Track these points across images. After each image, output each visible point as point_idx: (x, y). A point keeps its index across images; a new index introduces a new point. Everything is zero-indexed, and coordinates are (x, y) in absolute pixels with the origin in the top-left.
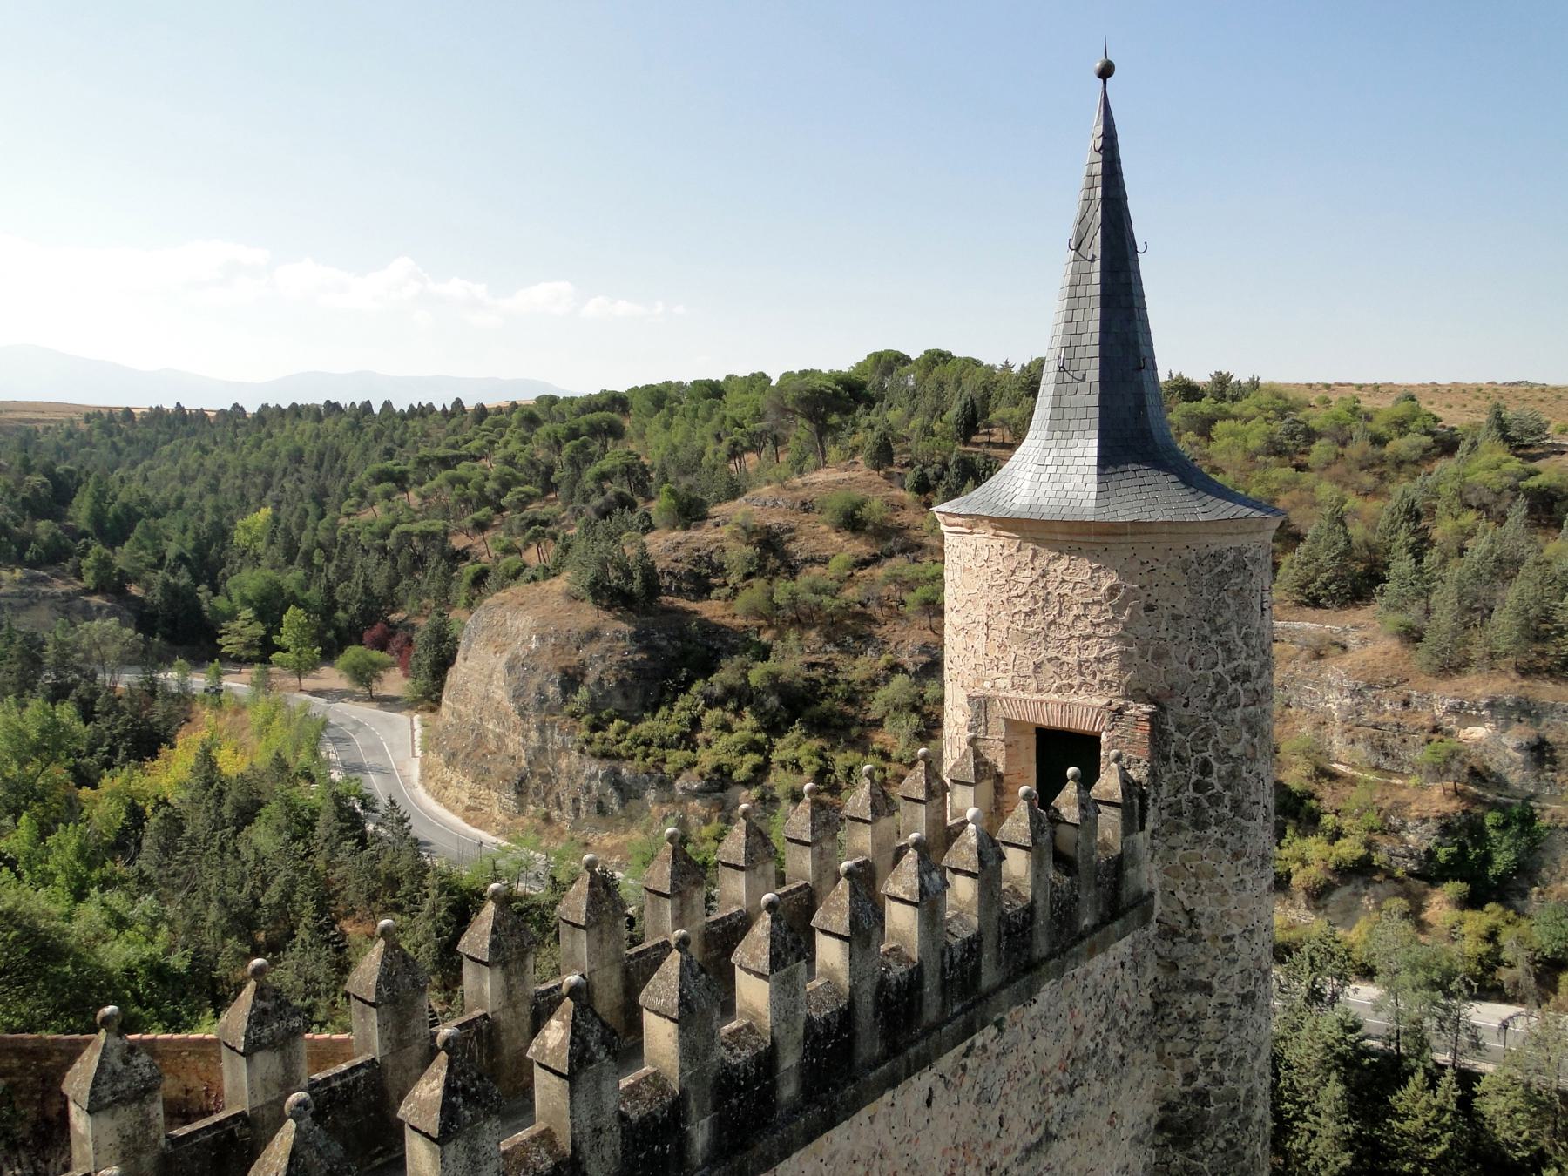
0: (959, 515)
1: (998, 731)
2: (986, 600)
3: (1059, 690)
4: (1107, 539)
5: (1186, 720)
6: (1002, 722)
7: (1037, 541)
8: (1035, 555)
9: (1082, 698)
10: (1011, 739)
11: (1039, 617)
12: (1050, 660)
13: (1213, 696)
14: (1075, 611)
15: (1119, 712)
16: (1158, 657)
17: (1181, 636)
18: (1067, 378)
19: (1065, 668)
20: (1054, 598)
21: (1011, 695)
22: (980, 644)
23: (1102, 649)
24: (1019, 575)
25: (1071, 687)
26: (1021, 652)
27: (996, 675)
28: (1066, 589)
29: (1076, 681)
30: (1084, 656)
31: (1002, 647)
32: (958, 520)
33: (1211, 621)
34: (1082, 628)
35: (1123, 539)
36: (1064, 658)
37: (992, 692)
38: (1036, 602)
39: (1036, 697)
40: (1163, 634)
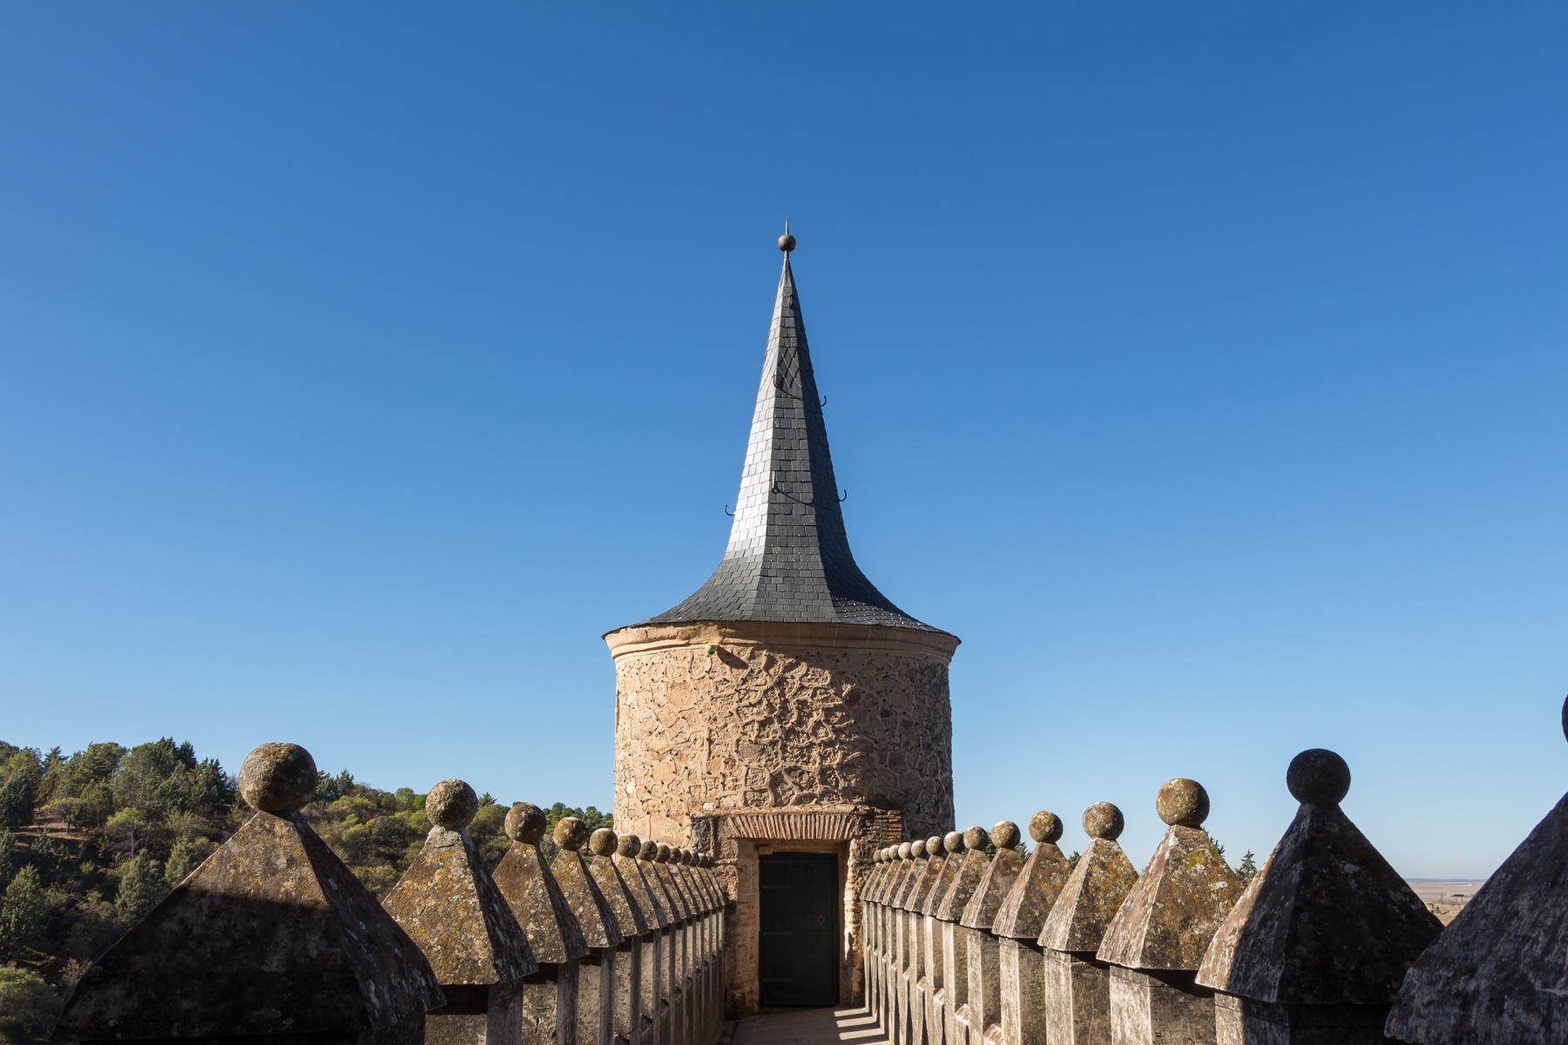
0: (675, 624)
1: (731, 849)
2: (707, 714)
3: (799, 802)
4: (848, 643)
5: (918, 826)
6: (735, 844)
7: (772, 648)
8: (771, 663)
9: (826, 806)
10: (741, 863)
11: (776, 726)
12: (789, 771)
13: (937, 802)
14: (815, 717)
15: (870, 816)
16: (895, 762)
17: (913, 743)
18: (781, 498)
19: (805, 777)
20: (792, 705)
21: (745, 810)
22: (698, 760)
23: (844, 756)
24: (751, 685)
25: (811, 797)
26: (754, 765)
27: (721, 793)
28: (806, 695)
29: (818, 789)
30: (827, 763)
31: (729, 762)
32: (671, 630)
33: (931, 729)
34: (825, 733)
35: (862, 644)
36: (804, 767)
37: (718, 812)
38: (771, 712)
39: (775, 810)
40: (897, 740)
